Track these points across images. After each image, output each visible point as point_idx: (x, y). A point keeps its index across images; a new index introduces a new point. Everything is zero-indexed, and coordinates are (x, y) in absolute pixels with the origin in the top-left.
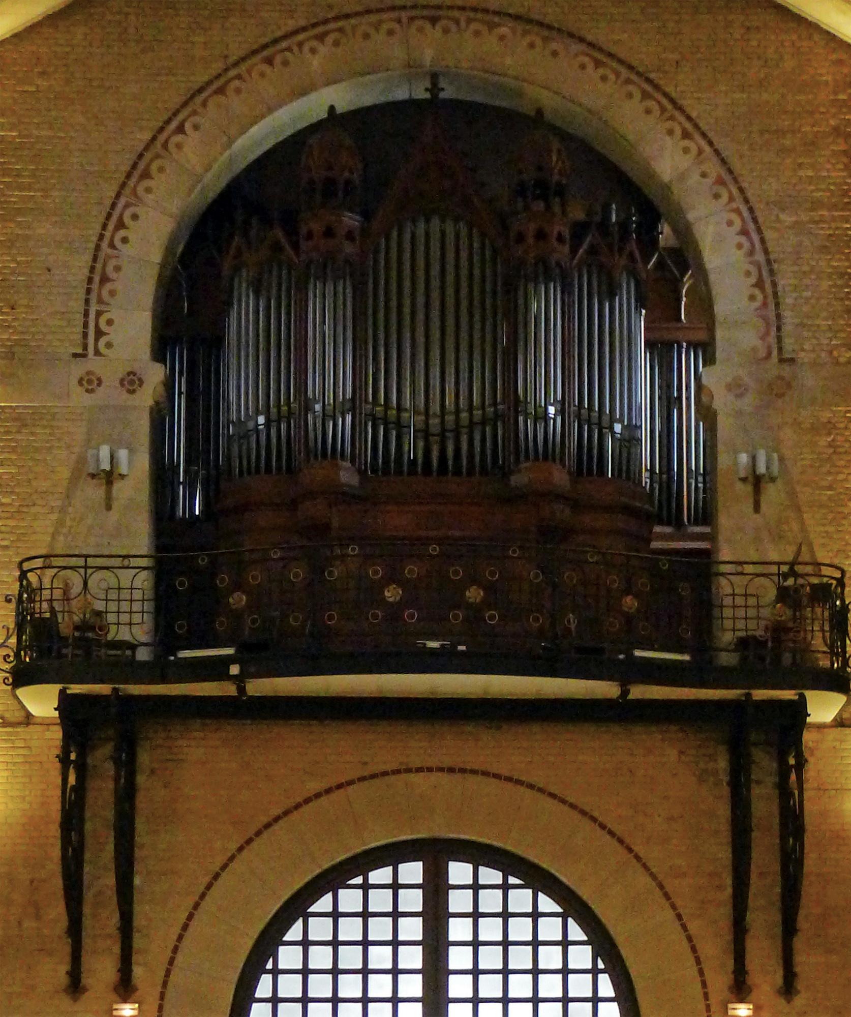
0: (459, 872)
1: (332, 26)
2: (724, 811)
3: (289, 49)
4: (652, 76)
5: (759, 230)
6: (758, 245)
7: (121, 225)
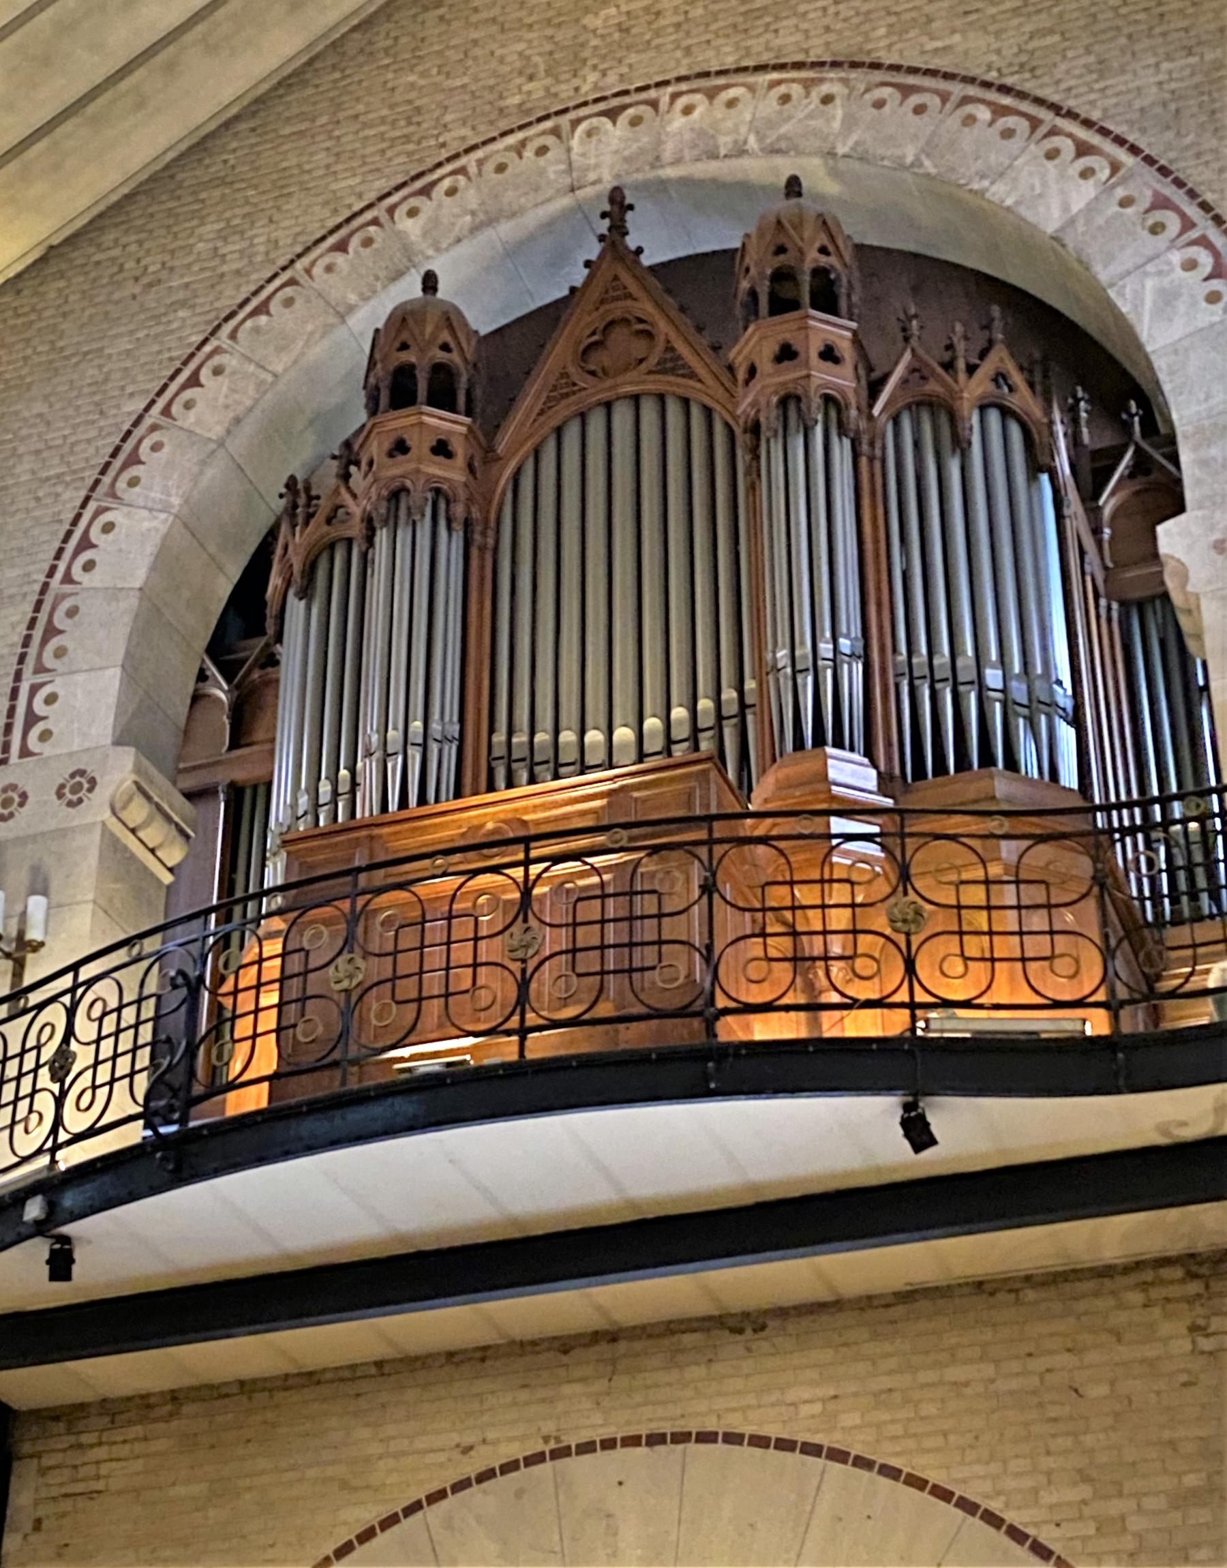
3: (375, 222)
4: (1009, 81)
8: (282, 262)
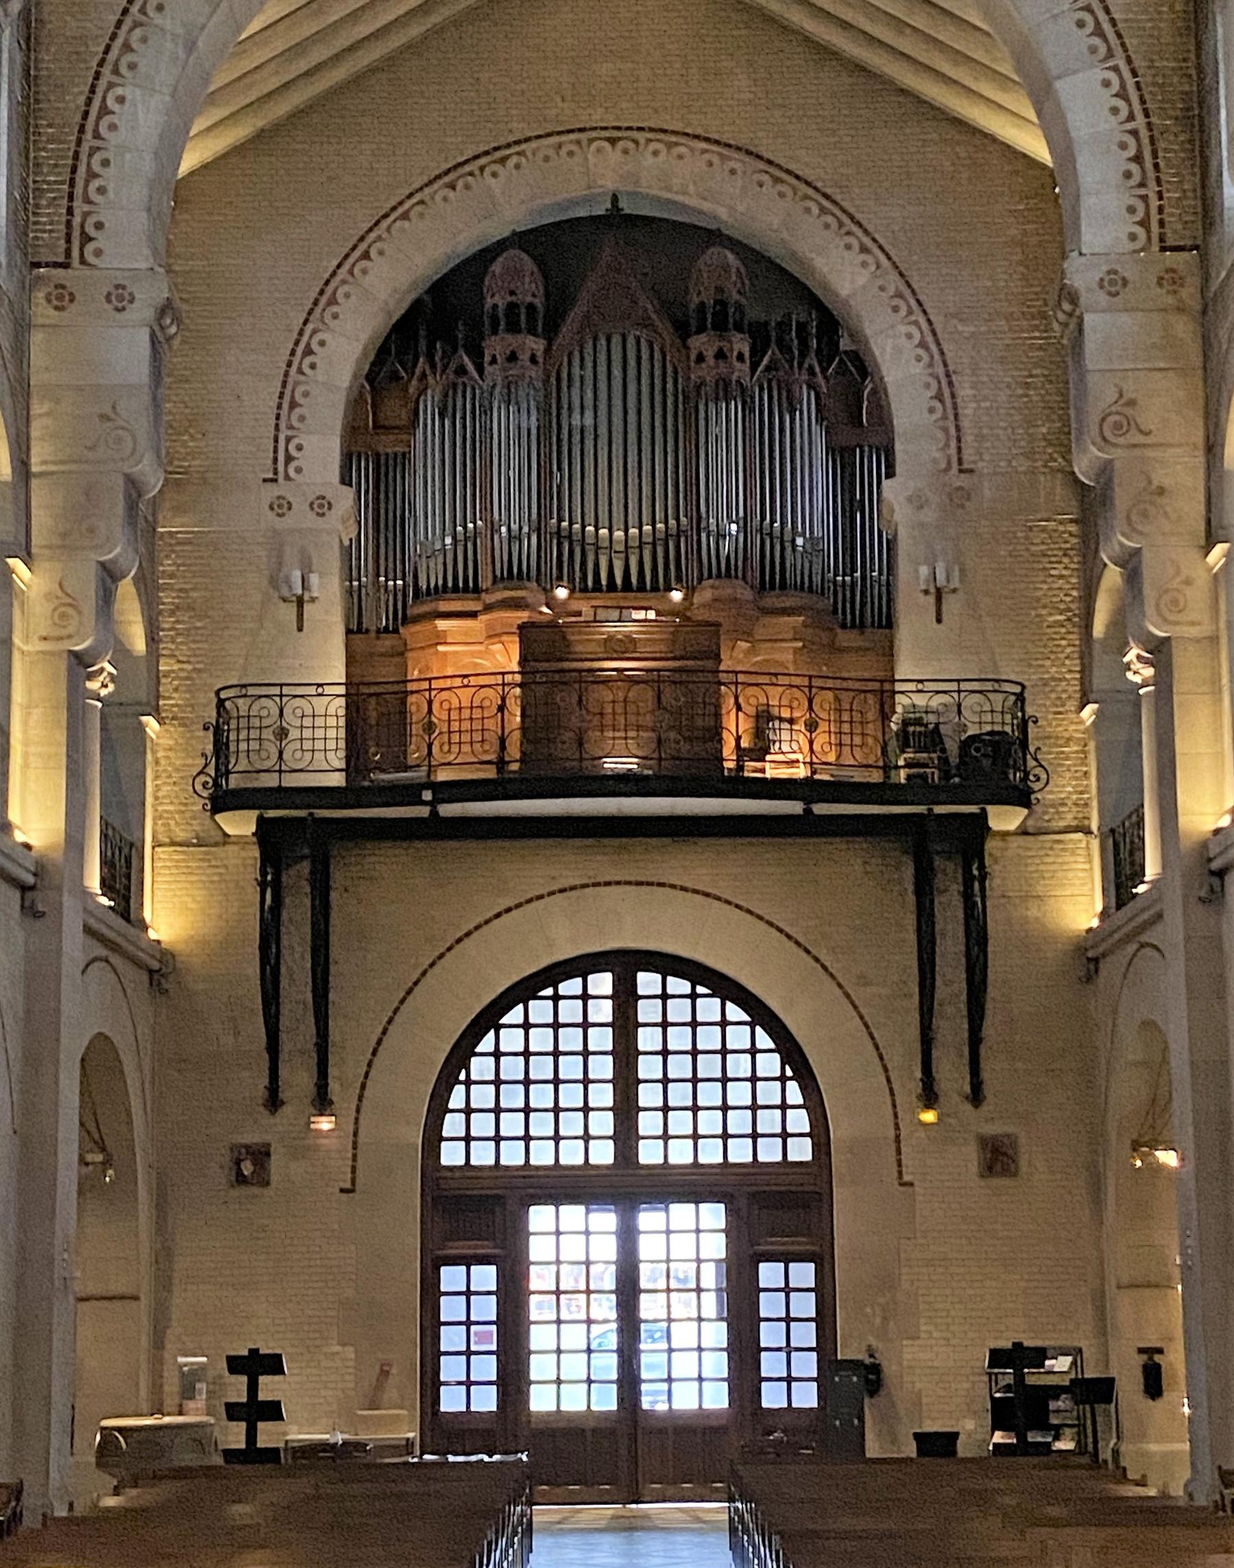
0: (647, 982)
1: (512, 151)
2: (911, 921)
3: (471, 174)
4: (829, 191)
5: (938, 344)
6: (937, 357)
7: (309, 351)
8: (416, 185)
